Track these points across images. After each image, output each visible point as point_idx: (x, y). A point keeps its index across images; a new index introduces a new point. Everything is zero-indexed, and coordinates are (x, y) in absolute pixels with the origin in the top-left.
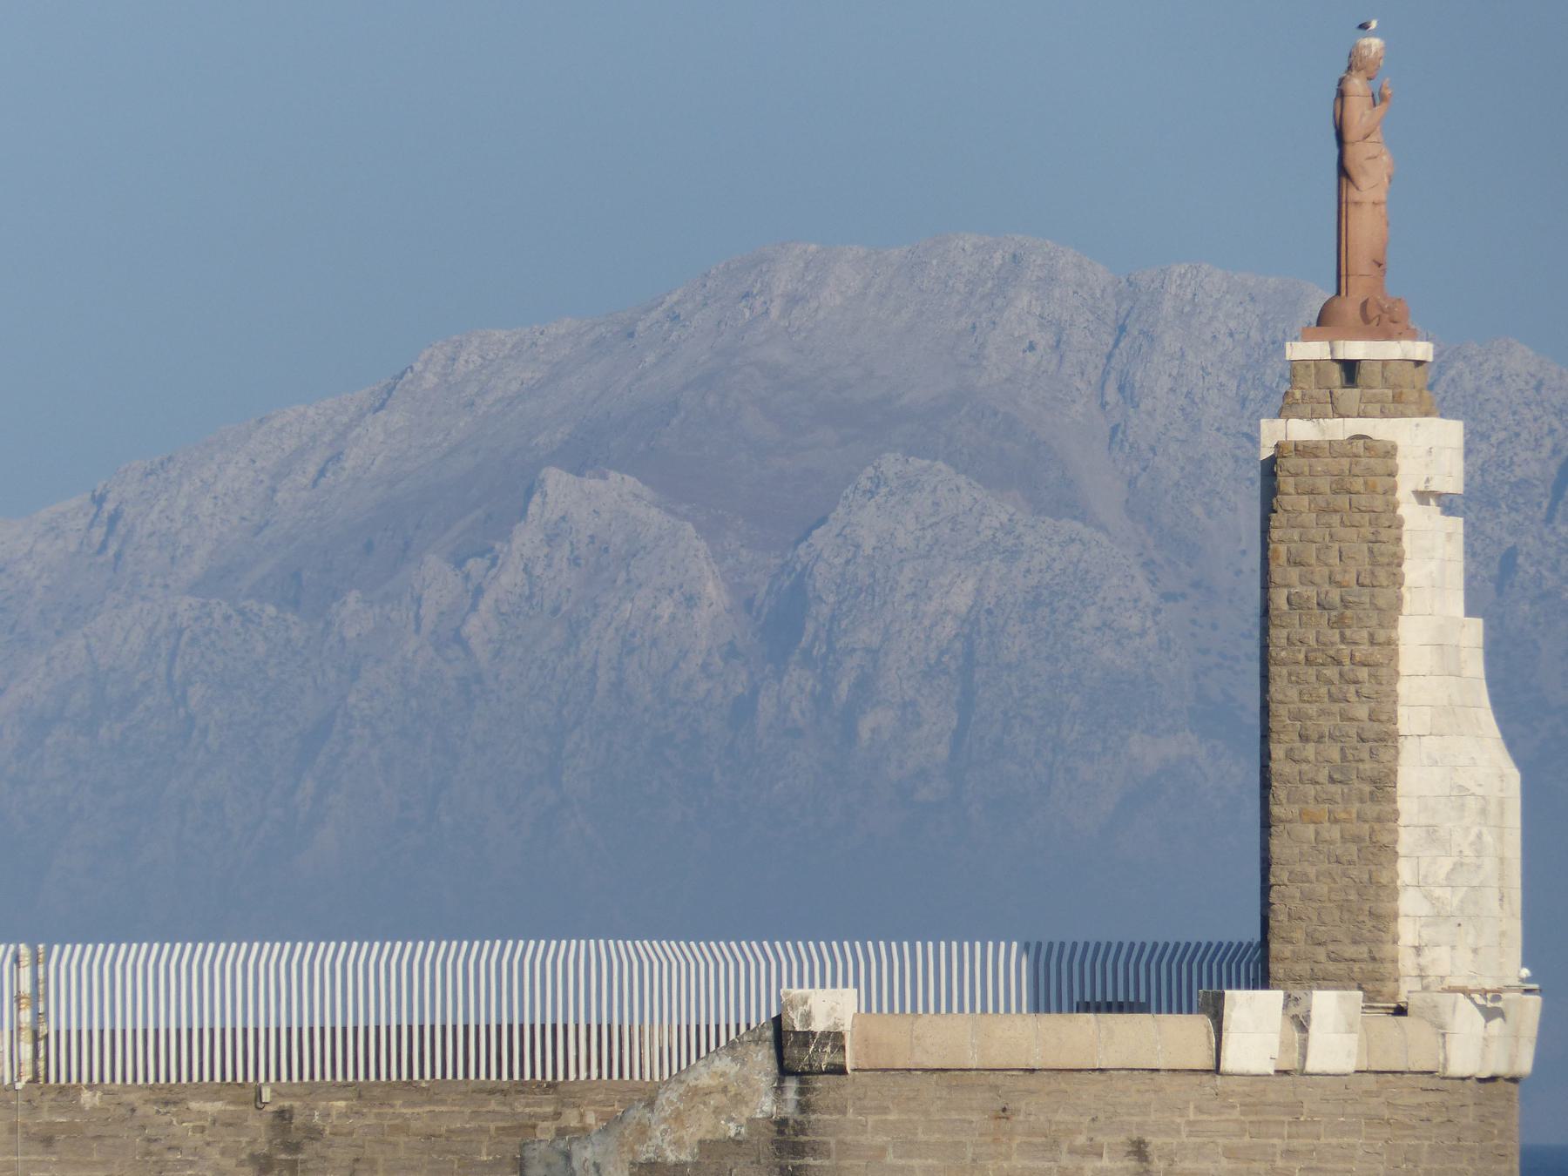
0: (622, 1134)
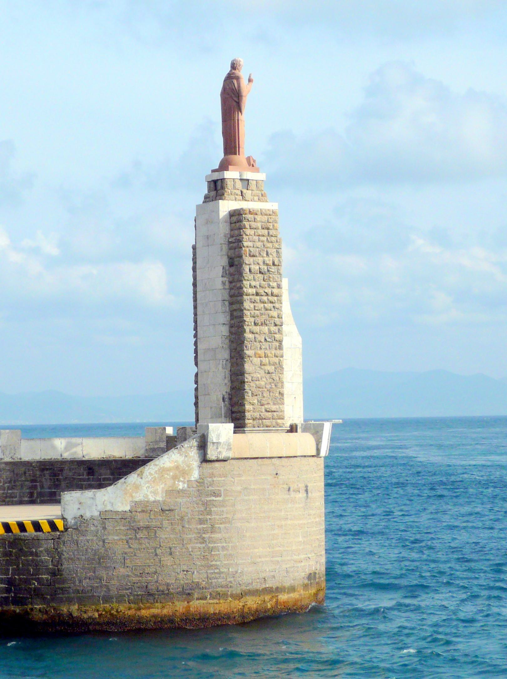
0: (126, 489)
